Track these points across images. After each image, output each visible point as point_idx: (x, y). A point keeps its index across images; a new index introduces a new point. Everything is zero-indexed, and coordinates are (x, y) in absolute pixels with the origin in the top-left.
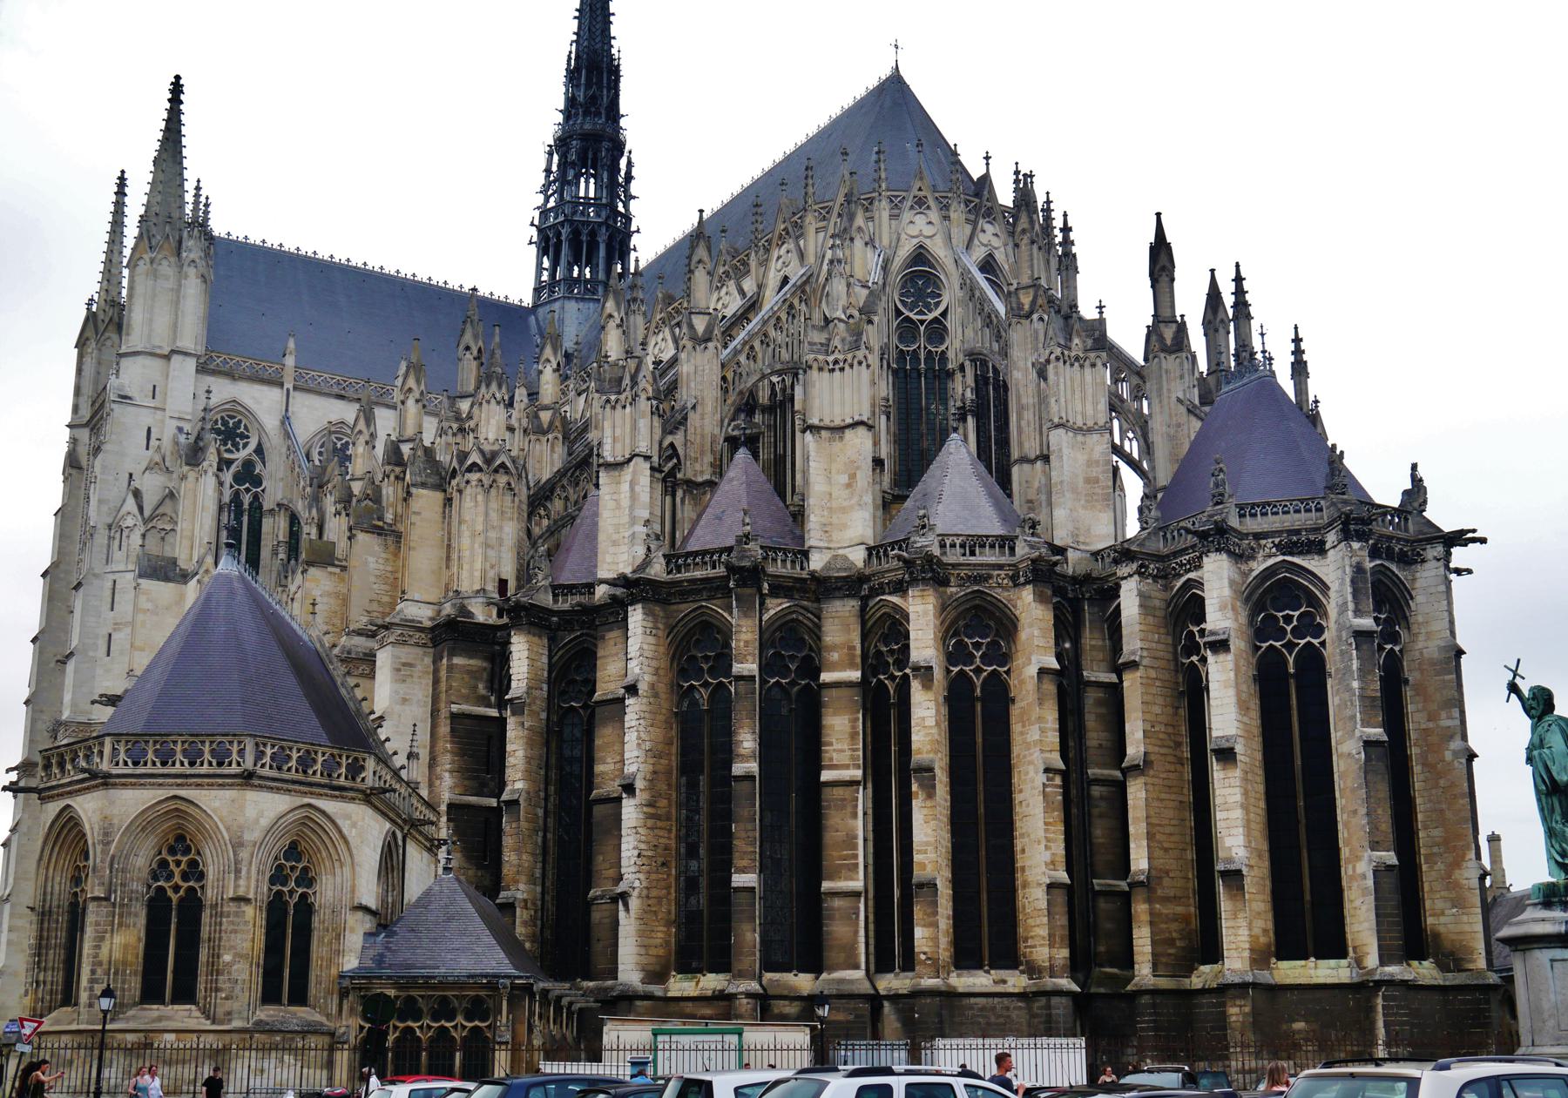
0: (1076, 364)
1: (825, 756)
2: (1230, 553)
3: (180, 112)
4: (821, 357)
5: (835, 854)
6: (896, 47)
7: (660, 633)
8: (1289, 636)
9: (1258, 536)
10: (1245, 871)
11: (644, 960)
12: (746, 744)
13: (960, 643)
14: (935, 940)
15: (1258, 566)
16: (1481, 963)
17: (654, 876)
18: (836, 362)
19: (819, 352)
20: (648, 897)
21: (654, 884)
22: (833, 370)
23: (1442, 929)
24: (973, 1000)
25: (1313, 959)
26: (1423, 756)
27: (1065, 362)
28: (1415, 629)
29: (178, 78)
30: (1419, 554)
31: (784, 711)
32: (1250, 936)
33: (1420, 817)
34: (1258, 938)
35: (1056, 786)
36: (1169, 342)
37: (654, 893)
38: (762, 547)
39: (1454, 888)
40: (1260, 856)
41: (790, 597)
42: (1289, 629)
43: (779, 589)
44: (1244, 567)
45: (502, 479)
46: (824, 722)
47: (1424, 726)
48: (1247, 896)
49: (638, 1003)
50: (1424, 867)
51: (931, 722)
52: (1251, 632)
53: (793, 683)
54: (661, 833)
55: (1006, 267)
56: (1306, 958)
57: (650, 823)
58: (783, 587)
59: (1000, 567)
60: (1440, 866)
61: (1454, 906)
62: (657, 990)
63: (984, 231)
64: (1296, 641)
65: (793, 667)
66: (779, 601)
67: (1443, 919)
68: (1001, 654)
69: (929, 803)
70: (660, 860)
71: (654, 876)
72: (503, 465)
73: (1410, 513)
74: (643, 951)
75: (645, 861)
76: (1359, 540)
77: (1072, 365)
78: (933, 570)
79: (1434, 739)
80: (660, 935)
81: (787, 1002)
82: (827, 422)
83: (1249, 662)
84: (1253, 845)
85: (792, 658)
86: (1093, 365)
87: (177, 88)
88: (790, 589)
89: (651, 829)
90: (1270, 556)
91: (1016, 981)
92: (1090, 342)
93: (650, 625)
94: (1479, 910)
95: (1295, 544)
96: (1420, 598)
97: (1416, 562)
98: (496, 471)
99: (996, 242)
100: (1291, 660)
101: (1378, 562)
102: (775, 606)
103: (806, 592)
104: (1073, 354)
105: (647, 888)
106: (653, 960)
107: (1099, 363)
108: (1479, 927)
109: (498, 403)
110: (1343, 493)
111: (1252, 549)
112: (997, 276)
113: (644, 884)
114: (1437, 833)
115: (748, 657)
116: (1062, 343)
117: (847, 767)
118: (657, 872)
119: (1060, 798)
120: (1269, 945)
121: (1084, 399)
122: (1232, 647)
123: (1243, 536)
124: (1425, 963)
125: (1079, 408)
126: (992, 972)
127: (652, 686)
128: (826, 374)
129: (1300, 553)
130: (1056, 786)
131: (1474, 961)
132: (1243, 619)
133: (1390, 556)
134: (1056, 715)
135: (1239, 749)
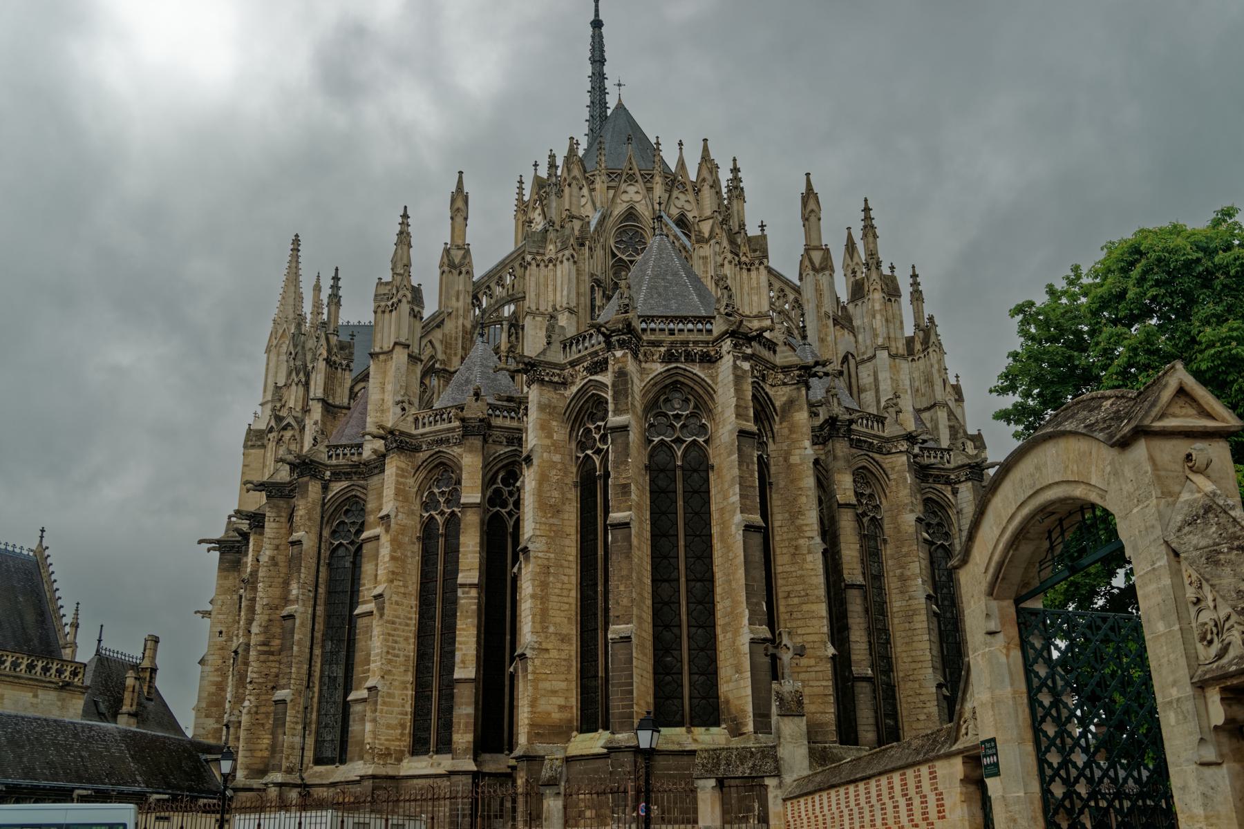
0: (551, 265)
1: (361, 594)
2: (542, 382)
3: (298, 257)
4: (383, 304)
5: (360, 669)
6: (619, 85)
7: (283, 520)
8: (598, 443)
9: (573, 364)
10: (529, 653)
11: (248, 761)
12: (294, 592)
13: (432, 493)
14: (375, 734)
15: (574, 389)
16: (750, 727)
17: (263, 697)
18: (393, 305)
19: (382, 300)
20: (256, 713)
21: (263, 703)
22: (391, 311)
23: (730, 696)
24: (415, 781)
25: (600, 731)
26: (722, 534)
27: (538, 265)
28: (717, 418)
29: (297, 236)
30: (717, 353)
31: (348, 564)
32: (532, 712)
33: (718, 590)
34: (549, 714)
35: (472, 598)
36: (707, 235)
37: (263, 710)
38: (327, 446)
39: (736, 652)
40: (564, 639)
41: (351, 479)
42: (597, 437)
43: (337, 476)
44: (567, 393)
45: (288, 434)
46: (363, 569)
47: (722, 506)
48: (530, 677)
49: (241, 794)
50: (720, 637)
51: (387, 559)
52: (574, 445)
53: (352, 543)
54: (273, 664)
55: (646, 213)
56: (596, 730)
57: (262, 657)
58: (344, 473)
59: (453, 430)
60: (729, 635)
61: (737, 672)
62: (256, 783)
63: (625, 192)
64: (601, 447)
65: (353, 530)
66: (342, 483)
67: (732, 685)
68: (453, 497)
69: (380, 622)
70: (270, 685)
71: (263, 697)
72: (289, 425)
73: (714, 318)
74: (248, 754)
75: (255, 686)
76: (621, 347)
77: (547, 266)
78: (396, 441)
79: (727, 516)
80: (266, 741)
81: (325, 789)
82: (386, 349)
83: (566, 472)
84: (552, 629)
85: (353, 523)
86: (562, 262)
87: (296, 241)
88: (348, 474)
89: (264, 662)
90: (583, 379)
91: (445, 763)
92: (559, 244)
93: (274, 515)
94: (749, 674)
95: (597, 362)
96: (720, 391)
97: (717, 360)
98: (284, 428)
99: (638, 198)
100: (598, 464)
101: (673, 365)
102: (337, 487)
103: (360, 474)
104: (546, 258)
105: (257, 707)
106: (258, 761)
107: (565, 261)
108: (749, 691)
109: (297, 384)
110: (626, 312)
111: (572, 376)
112: (641, 222)
113: (253, 704)
114: (727, 603)
115: (302, 528)
116: (535, 251)
117: (369, 602)
118: (267, 693)
119: (475, 607)
120: (570, 721)
121: (555, 290)
122: (535, 461)
123: (563, 367)
124: (714, 730)
125: (551, 298)
126: (435, 757)
127: (272, 558)
128: (387, 315)
129: (602, 371)
130: (472, 598)
131: (746, 725)
132: (560, 432)
133: (689, 358)
134: (478, 540)
135: (531, 546)
